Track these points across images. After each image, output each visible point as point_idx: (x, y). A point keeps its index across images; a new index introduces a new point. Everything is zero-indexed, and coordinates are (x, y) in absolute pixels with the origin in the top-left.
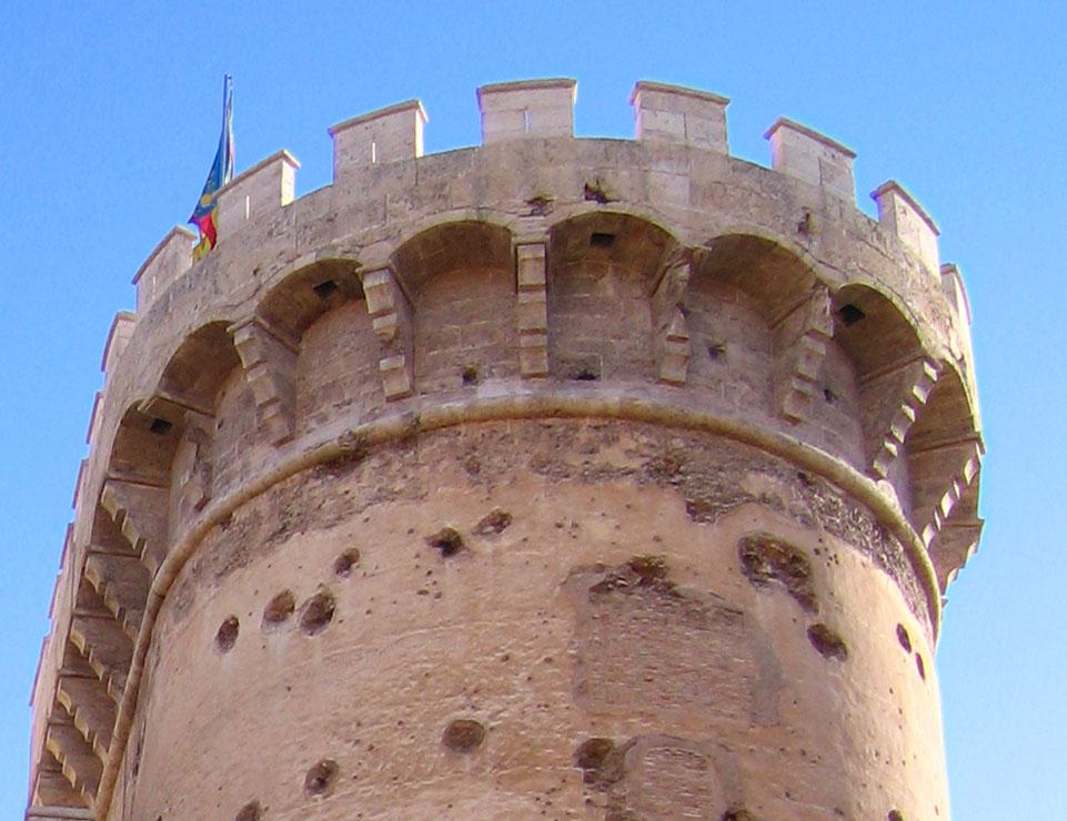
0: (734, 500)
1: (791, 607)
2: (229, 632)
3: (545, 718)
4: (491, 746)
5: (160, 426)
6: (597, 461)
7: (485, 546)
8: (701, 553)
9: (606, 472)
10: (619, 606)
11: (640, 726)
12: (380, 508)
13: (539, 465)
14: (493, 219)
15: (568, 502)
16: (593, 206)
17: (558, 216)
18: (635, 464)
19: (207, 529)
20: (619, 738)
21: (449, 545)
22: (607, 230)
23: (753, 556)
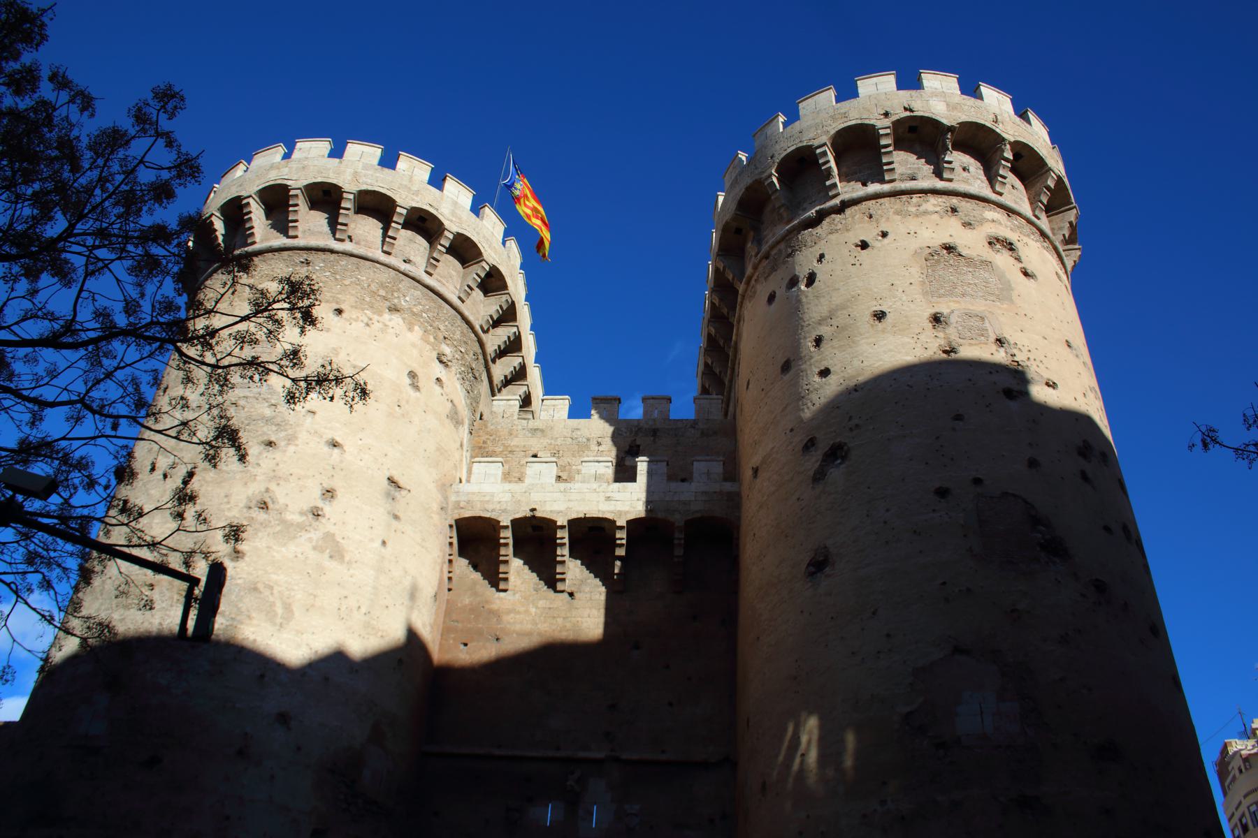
0: (983, 221)
1: (1012, 260)
2: (771, 298)
3: (912, 306)
4: (889, 319)
5: (738, 231)
6: (921, 209)
7: (877, 244)
8: (971, 242)
9: (926, 213)
10: (938, 261)
11: (953, 306)
12: (830, 236)
13: (898, 213)
14: (867, 122)
15: (912, 224)
16: (908, 114)
17: (894, 118)
18: (938, 209)
19: (760, 261)
20: (945, 311)
21: (864, 245)
22: (914, 124)
23: (994, 242)
